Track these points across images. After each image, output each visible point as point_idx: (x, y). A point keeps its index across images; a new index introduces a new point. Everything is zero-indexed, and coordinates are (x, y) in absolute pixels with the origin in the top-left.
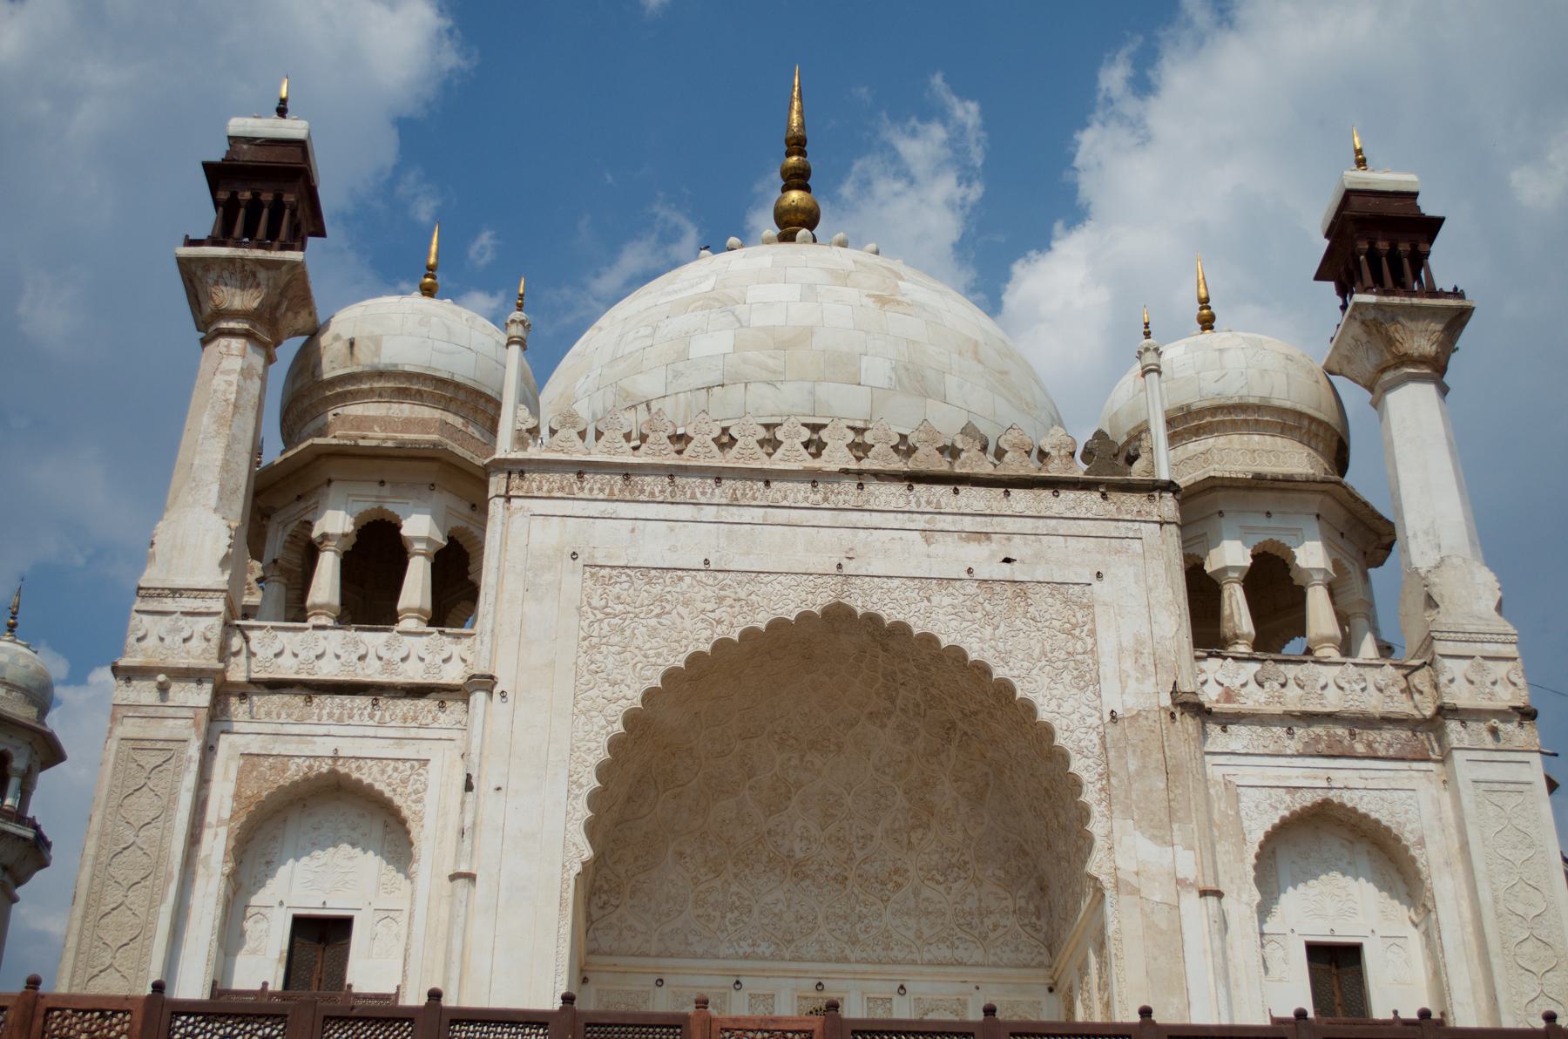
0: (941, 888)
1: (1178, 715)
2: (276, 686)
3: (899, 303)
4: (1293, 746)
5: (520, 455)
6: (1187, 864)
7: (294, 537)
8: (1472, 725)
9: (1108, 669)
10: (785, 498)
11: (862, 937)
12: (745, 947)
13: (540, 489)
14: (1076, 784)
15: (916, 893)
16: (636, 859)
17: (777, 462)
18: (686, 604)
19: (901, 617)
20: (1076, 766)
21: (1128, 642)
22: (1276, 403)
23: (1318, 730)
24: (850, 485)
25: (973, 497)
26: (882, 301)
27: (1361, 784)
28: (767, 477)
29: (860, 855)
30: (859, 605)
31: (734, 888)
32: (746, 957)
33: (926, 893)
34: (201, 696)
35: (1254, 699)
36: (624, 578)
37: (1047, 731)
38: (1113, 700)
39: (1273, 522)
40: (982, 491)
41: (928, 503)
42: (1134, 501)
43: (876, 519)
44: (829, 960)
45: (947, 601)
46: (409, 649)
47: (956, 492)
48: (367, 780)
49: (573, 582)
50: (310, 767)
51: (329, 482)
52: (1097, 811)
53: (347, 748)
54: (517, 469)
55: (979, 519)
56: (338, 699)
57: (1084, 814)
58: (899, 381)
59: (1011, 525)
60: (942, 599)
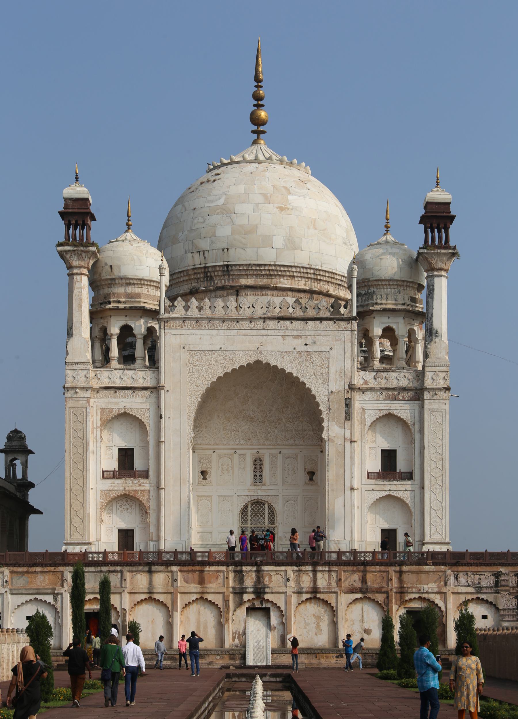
0: (292, 424)
1: (350, 391)
3: (287, 209)
4: (382, 397)
5: (166, 316)
7: (101, 329)
8: (431, 393)
10: (243, 327)
11: (269, 438)
12: (237, 442)
13: (173, 326)
14: (321, 412)
15: (285, 426)
16: (206, 418)
18: (216, 361)
19: (275, 364)
20: (321, 407)
21: (338, 370)
22: (396, 278)
23: (390, 393)
24: (261, 321)
25: (297, 324)
27: (399, 408)
28: (237, 320)
29: (269, 415)
30: (264, 360)
31: (234, 425)
32: (238, 445)
33: (287, 425)
36: (198, 354)
37: (314, 397)
38: (332, 388)
39: (390, 320)
40: (300, 322)
41: (284, 327)
42: (343, 324)
43: (269, 332)
44: (260, 445)
45: (288, 358)
47: (292, 323)
48: (134, 414)
49: (186, 356)
50: (119, 411)
51: (111, 316)
52: (326, 419)
53: (128, 405)
54: (167, 320)
55: (298, 331)
56: (123, 391)
57: (322, 420)
58: (286, 245)
59: (308, 333)
60: (287, 357)
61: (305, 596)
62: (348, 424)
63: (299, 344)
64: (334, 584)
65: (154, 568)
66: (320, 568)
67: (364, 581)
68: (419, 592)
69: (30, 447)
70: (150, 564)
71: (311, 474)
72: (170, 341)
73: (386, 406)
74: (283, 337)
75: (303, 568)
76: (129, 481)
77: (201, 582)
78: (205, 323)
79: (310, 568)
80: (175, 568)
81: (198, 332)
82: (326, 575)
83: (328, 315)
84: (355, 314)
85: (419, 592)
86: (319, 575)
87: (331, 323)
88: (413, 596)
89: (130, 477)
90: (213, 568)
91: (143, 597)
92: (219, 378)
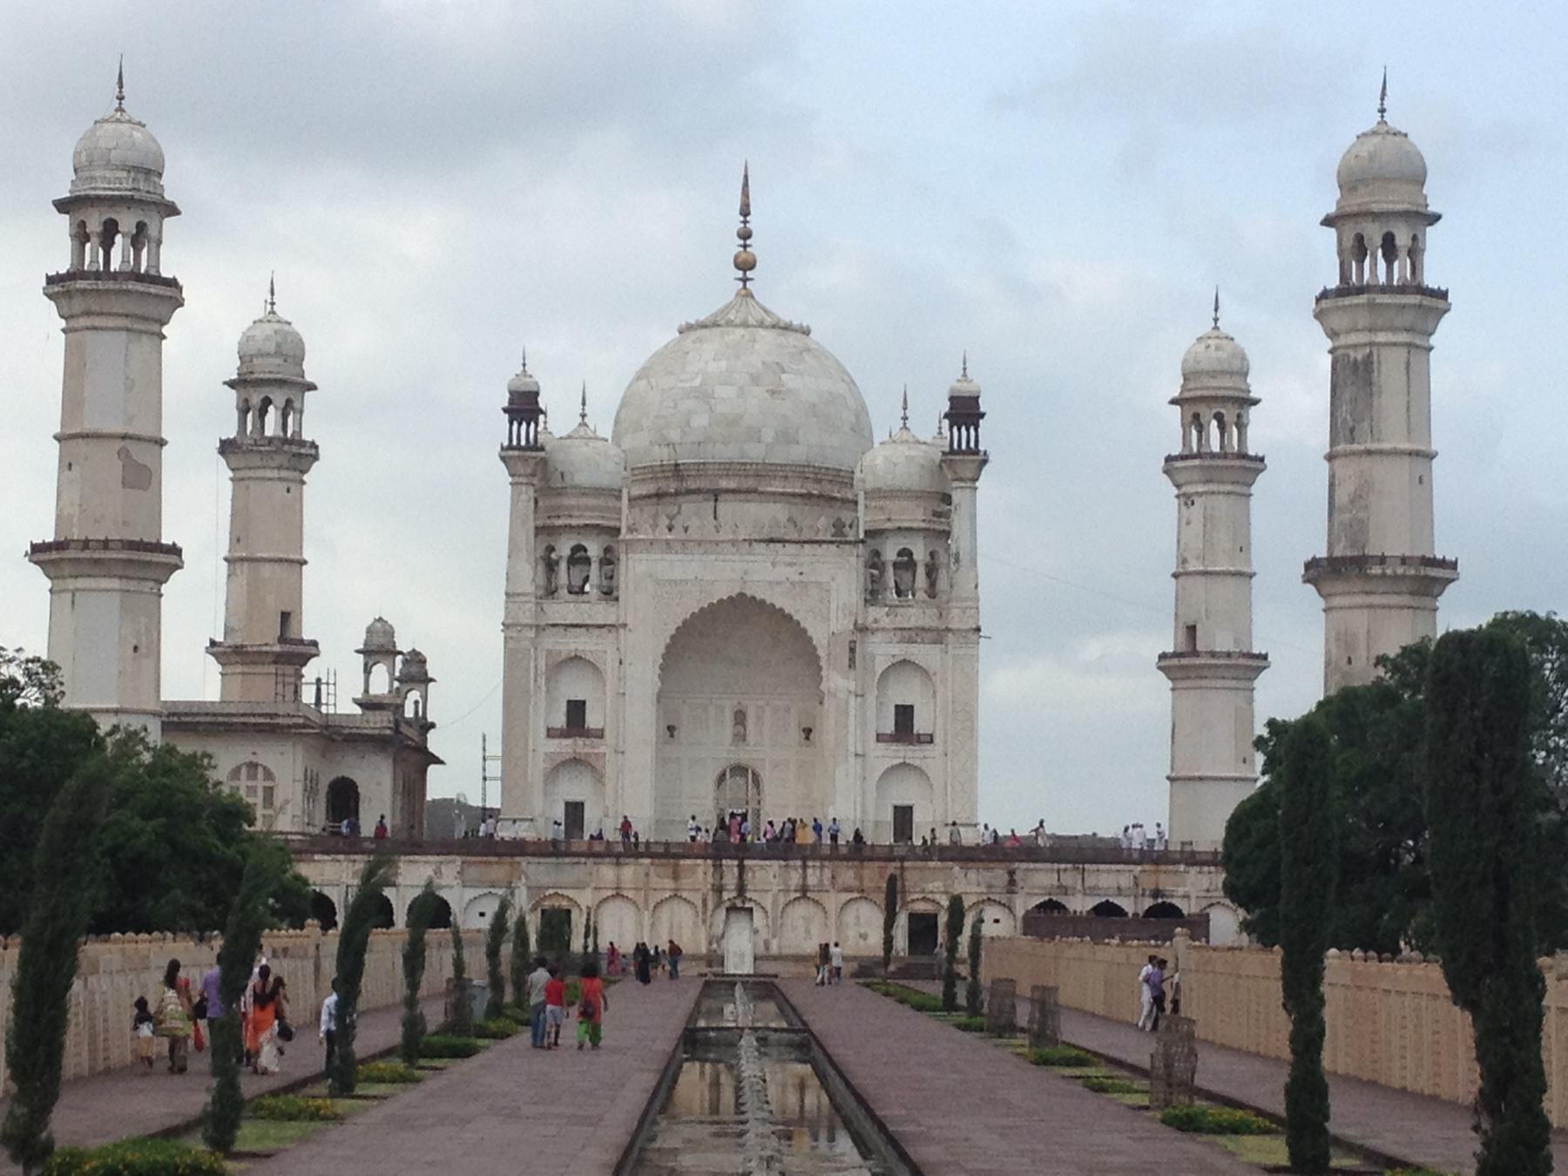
2: (554, 625)
6: (852, 686)
9: (833, 615)
14: (818, 657)
17: (722, 536)
23: (906, 634)
25: (791, 548)
26: (773, 393)
30: (749, 593)
34: (532, 634)
35: (886, 622)
38: (834, 627)
42: (847, 547)
46: (595, 610)
54: (628, 543)
57: (820, 668)
60: (778, 589)
61: (793, 895)
62: (852, 674)
63: (791, 573)
64: (826, 882)
65: (622, 860)
66: (810, 863)
67: (861, 880)
68: (923, 891)
69: (430, 675)
70: (618, 856)
71: (808, 732)
72: (634, 568)
73: (899, 650)
74: (774, 564)
75: (791, 863)
76: (580, 741)
77: (676, 877)
78: (678, 546)
79: (799, 863)
80: (647, 861)
81: (668, 557)
82: (818, 872)
83: (829, 538)
84: (861, 536)
85: (923, 891)
86: (810, 871)
87: (833, 547)
88: (915, 896)
89: (581, 736)
90: (689, 862)
91: (610, 893)
92: (693, 615)
